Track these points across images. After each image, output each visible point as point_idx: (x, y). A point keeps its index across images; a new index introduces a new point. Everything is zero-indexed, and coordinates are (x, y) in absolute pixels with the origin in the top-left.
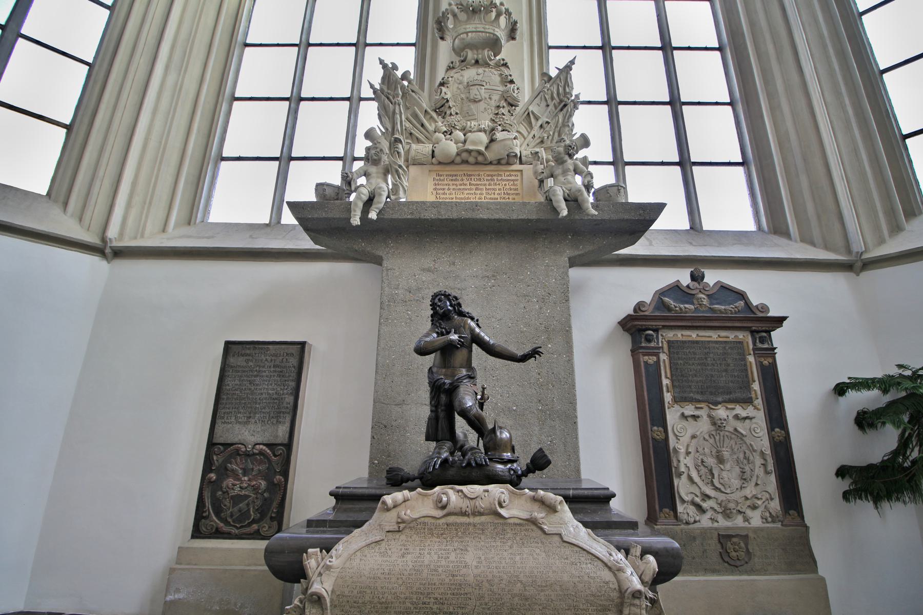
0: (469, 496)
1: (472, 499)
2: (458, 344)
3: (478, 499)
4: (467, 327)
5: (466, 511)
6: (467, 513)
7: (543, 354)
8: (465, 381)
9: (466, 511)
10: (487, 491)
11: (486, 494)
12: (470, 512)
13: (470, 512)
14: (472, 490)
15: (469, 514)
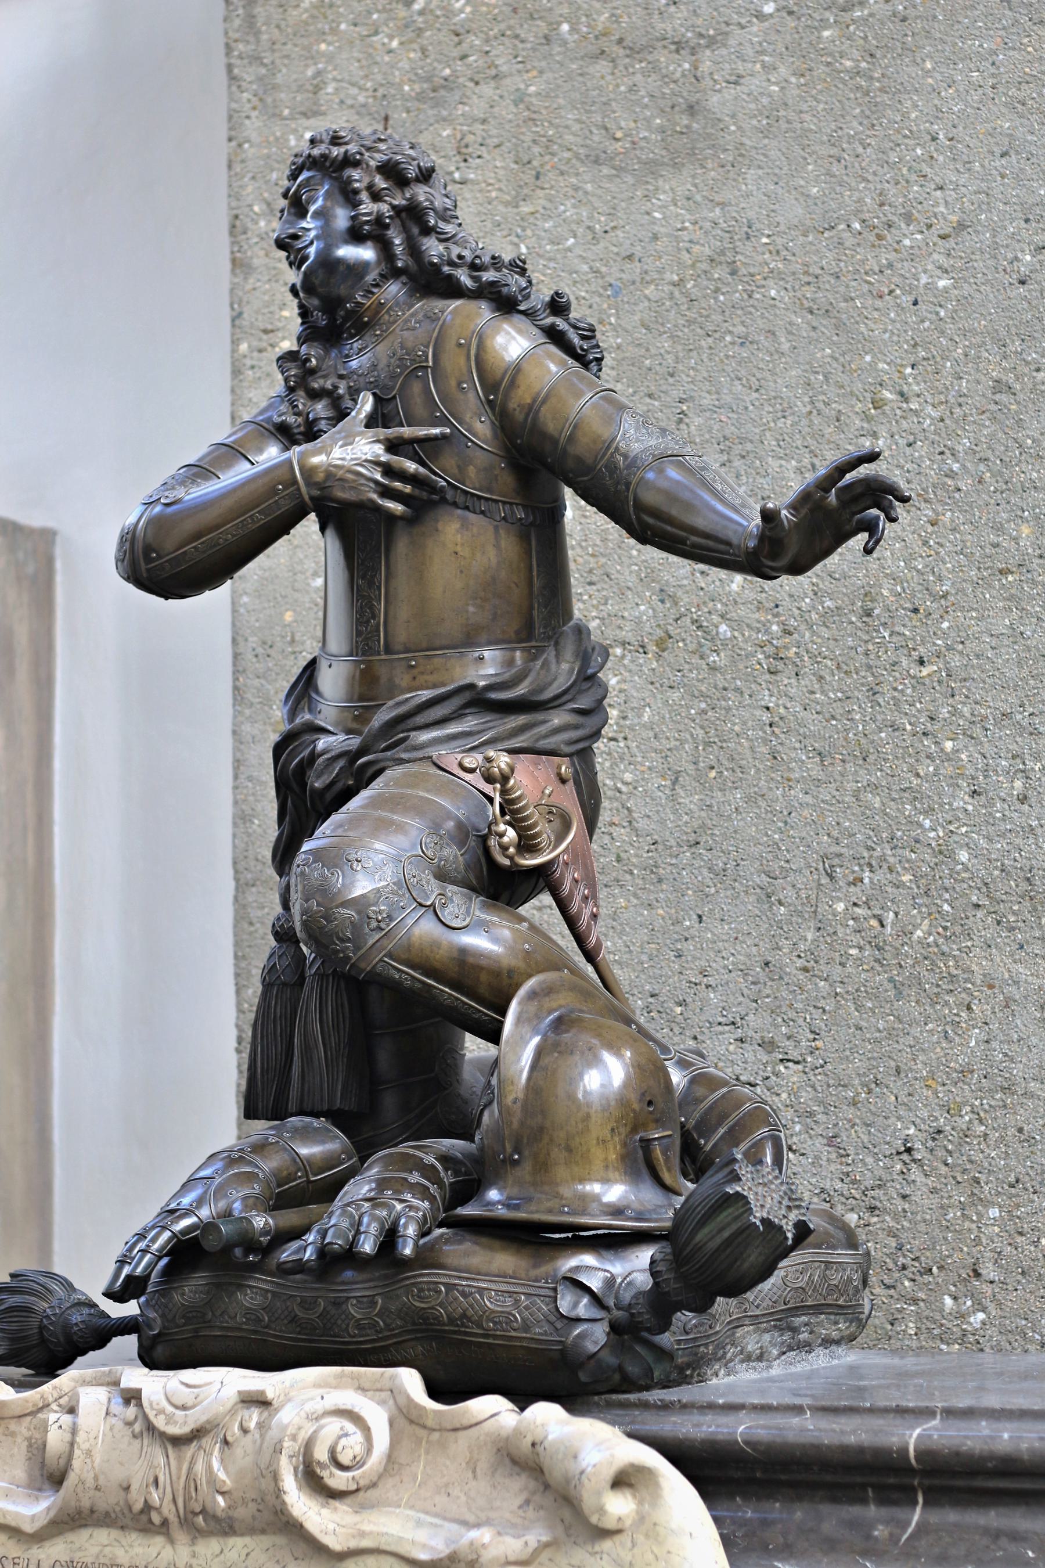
0: (160, 1423)
1: (178, 1441)
2: (387, 492)
3: (206, 1442)
4: (455, 363)
5: (148, 1507)
6: (156, 1519)
7: (905, 500)
8: (425, 736)
9: (148, 1507)
10: (259, 1401)
11: (253, 1417)
12: (168, 1510)
13: (168, 1510)
14: (185, 1395)
15: (165, 1523)
